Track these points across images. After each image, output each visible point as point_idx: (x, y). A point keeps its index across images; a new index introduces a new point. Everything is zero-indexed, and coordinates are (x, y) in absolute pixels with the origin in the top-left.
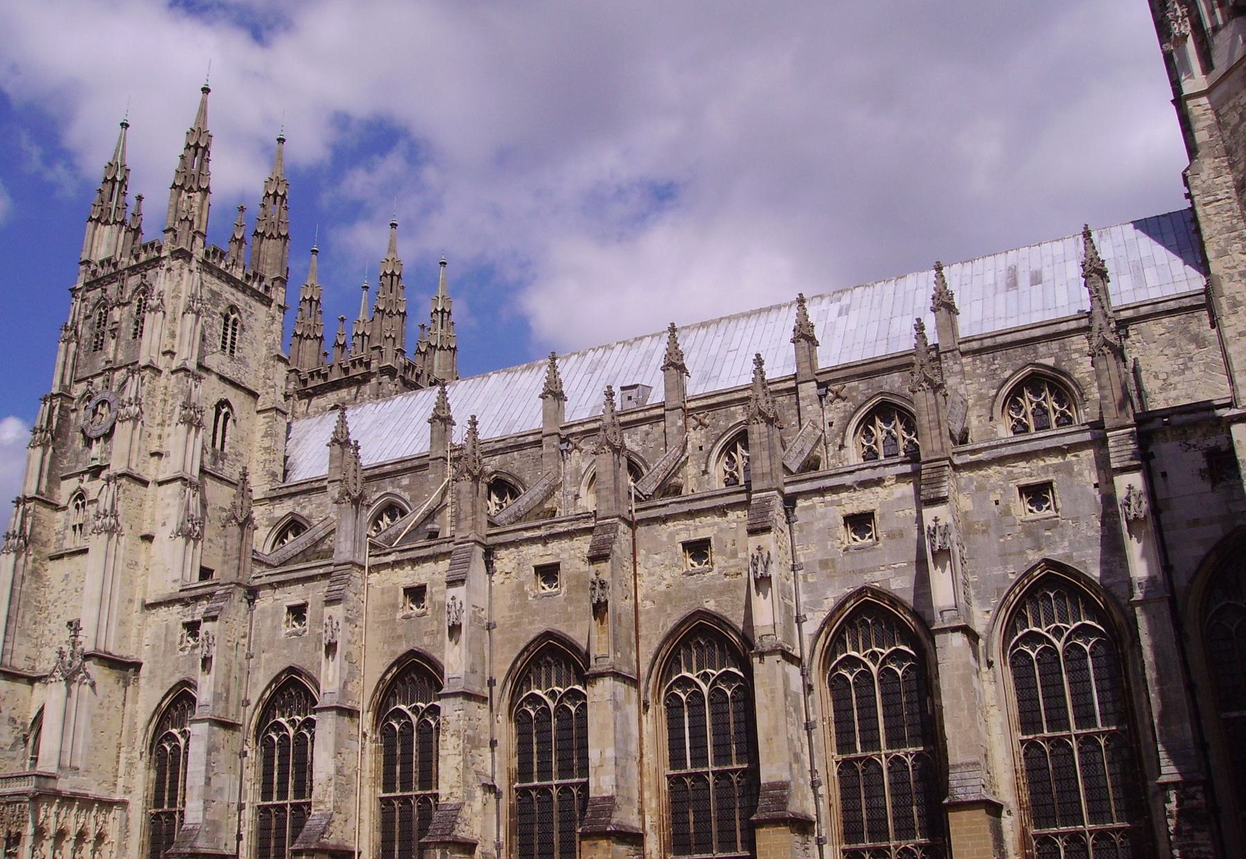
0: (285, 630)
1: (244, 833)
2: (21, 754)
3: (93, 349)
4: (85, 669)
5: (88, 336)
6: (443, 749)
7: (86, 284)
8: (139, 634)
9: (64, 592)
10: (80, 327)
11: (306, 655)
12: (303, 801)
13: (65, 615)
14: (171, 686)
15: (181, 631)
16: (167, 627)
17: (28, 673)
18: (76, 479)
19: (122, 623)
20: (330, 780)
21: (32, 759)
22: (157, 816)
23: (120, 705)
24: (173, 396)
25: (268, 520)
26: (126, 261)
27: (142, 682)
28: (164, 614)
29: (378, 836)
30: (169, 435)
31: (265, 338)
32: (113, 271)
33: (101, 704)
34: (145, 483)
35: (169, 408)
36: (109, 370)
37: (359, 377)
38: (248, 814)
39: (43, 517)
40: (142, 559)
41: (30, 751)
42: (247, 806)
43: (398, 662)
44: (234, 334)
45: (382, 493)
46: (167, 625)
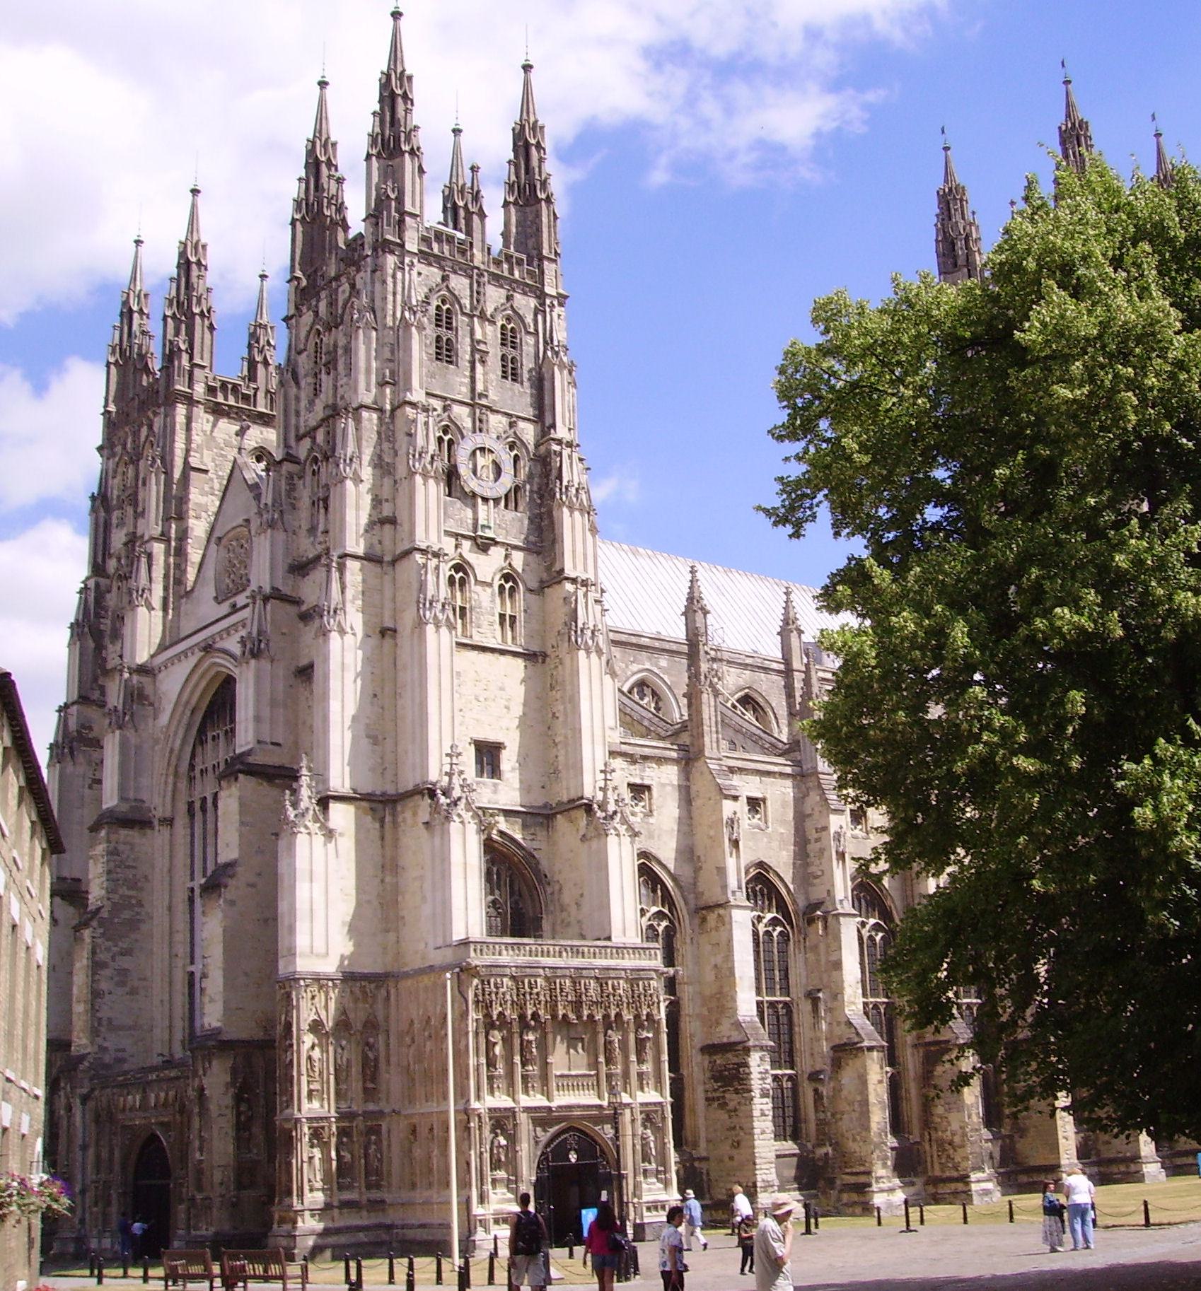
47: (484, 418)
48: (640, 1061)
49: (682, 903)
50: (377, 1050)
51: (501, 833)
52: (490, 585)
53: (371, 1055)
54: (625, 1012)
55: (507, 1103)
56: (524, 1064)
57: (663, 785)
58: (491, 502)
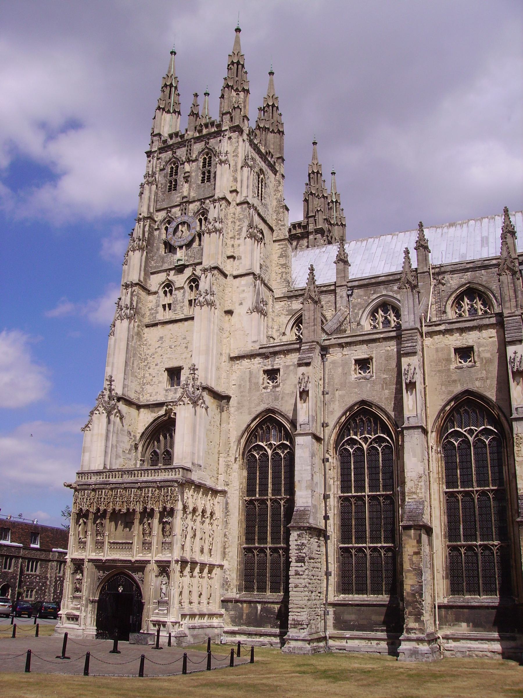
0: (354, 376)
1: (331, 514)
2: (134, 457)
3: (168, 190)
4: (203, 397)
5: (164, 182)
6: (518, 456)
7: (159, 149)
8: (228, 378)
9: (160, 349)
10: (157, 176)
11: (375, 393)
12: (378, 493)
13: (162, 364)
14: (258, 412)
15: (262, 377)
16: (251, 373)
17: (136, 401)
18: (164, 274)
19: (218, 369)
20: (420, 477)
21: (141, 460)
22: (251, 502)
23: (219, 425)
24: (240, 220)
25: (287, 311)
26: (191, 134)
27: (232, 410)
28: (247, 364)
29: (445, 518)
30: (239, 245)
31: (275, 195)
32: (180, 140)
33: (210, 423)
34: (225, 276)
35: (237, 228)
36: (186, 202)
37: (299, 235)
38: (333, 502)
39: (142, 298)
40: (226, 326)
41: (139, 455)
42: (332, 496)
43: (455, 398)
44: (262, 188)
45: (379, 295)
46: (250, 371)
57: (288, 367)
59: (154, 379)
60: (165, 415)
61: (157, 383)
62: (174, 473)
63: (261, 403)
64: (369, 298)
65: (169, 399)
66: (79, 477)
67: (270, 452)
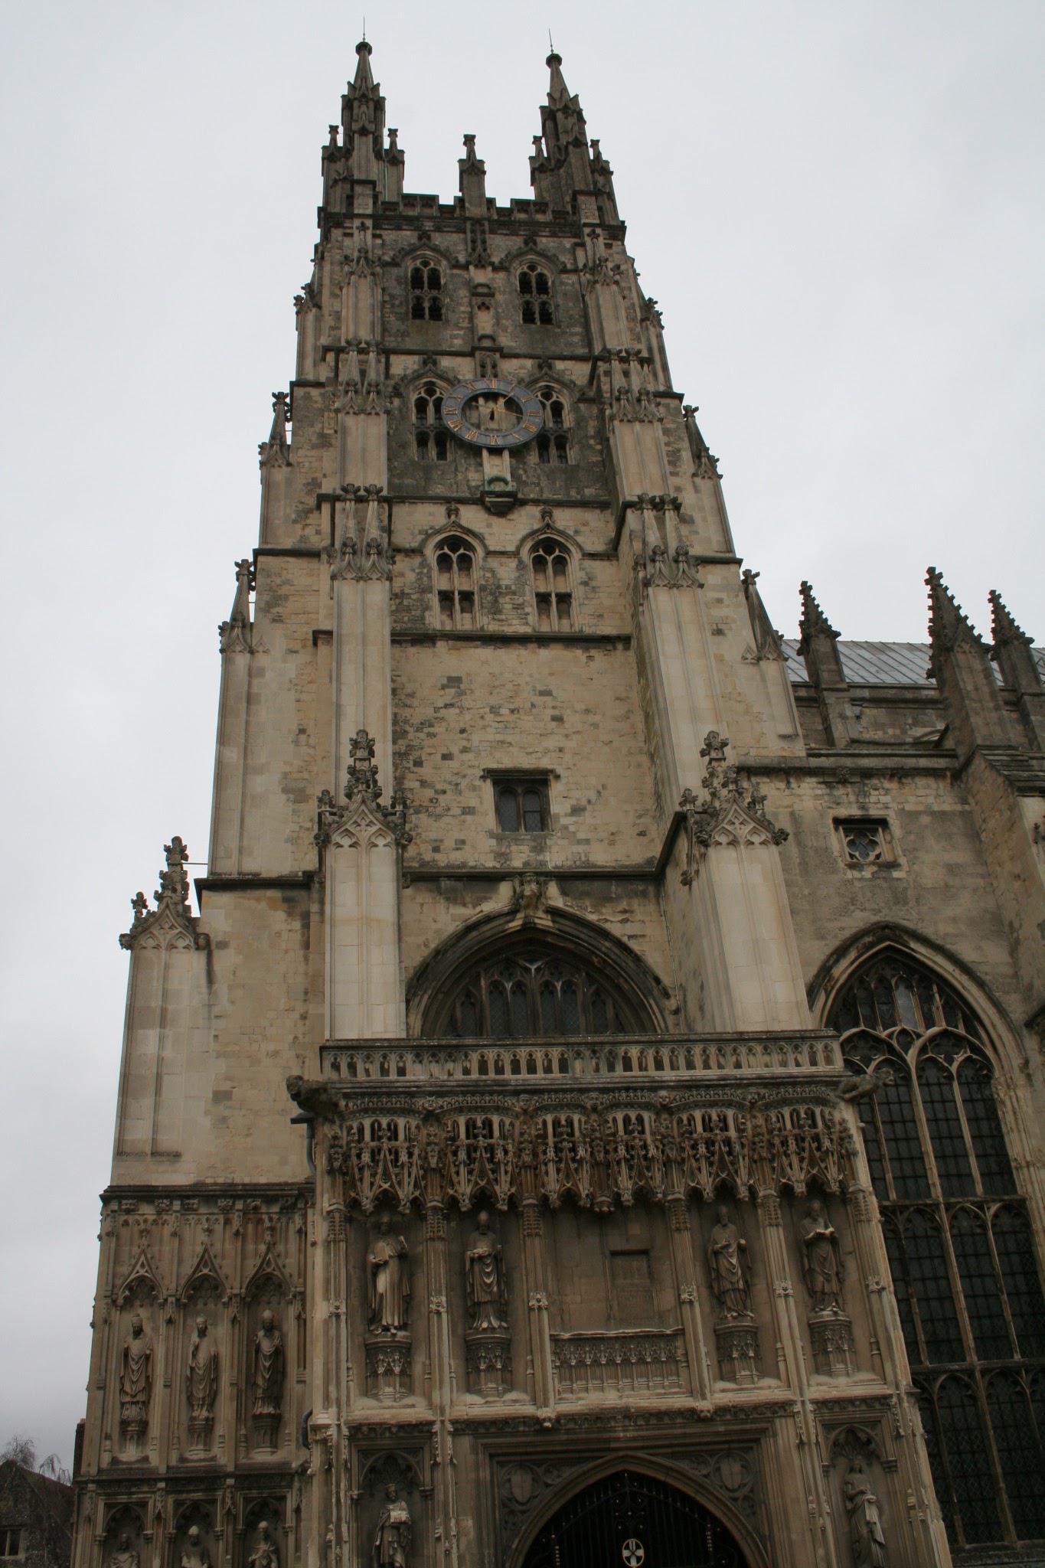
9: (453, 711)
14: (847, 934)
28: (777, 793)
45: (928, 730)
47: (488, 361)
48: (815, 1297)
49: (992, 1011)
50: (283, 1337)
51: (554, 912)
52: (516, 554)
53: (267, 1346)
54: (742, 1181)
55: (415, 1410)
56: (471, 1311)
57: (914, 815)
58: (506, 454)
59: (441, 798)
60: (512, 913)
61: (457, 811)
62: (804, 1058)
63: (852, 908)
64: (904, 732)
65: (517, 863)
66: (336, 1067)
67: (911, 1057)
